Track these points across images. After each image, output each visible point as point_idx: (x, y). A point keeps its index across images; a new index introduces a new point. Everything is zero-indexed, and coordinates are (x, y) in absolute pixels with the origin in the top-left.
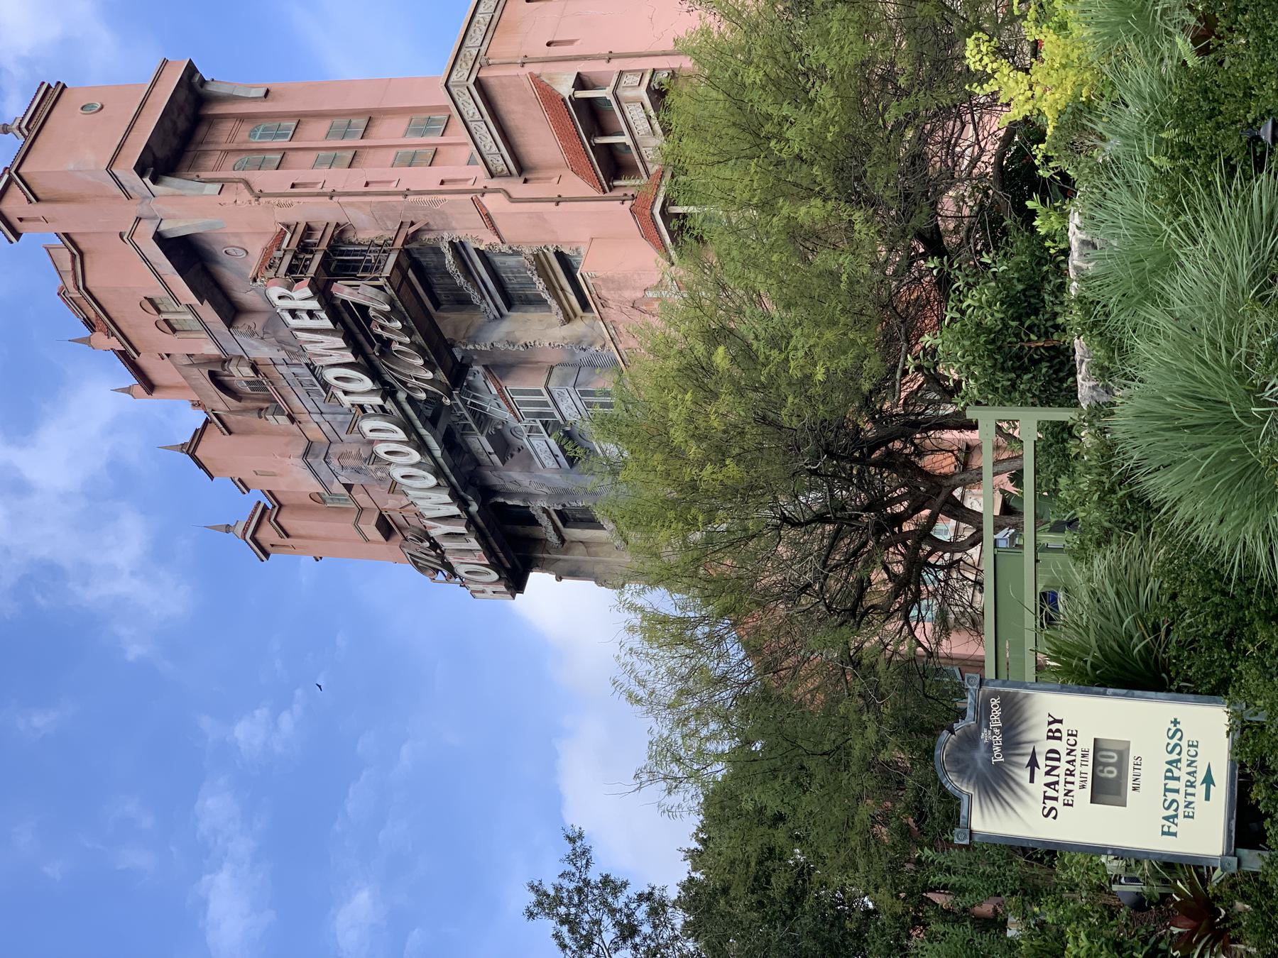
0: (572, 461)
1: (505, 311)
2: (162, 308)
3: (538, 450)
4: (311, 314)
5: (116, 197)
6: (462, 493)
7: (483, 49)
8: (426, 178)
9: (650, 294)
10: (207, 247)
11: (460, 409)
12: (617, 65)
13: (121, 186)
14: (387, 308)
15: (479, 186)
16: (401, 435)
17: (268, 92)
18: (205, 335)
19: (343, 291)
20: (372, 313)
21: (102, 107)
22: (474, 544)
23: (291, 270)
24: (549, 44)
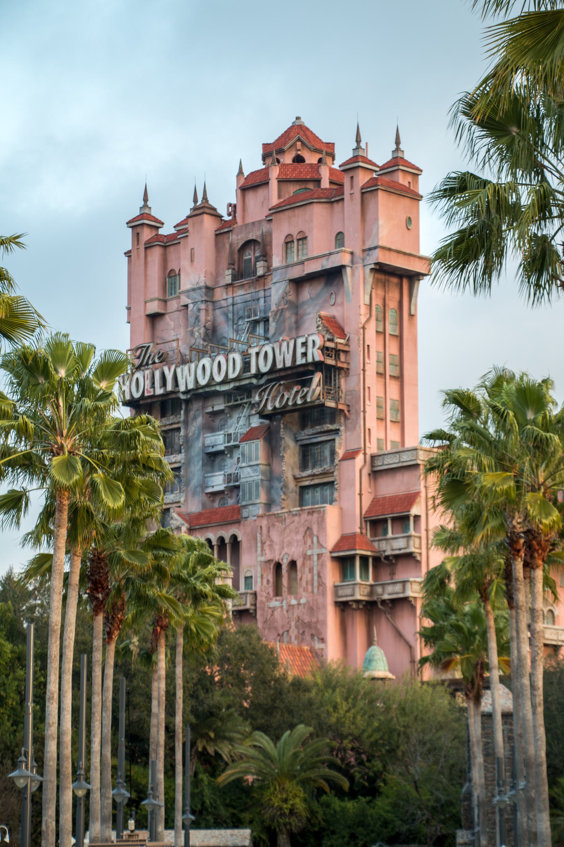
0: (208, 454)
1: (299, 443)
2: (300, 242)
3: (216, 437)
4: (305, 354)
5: (364, 242)
6: (192, 393)
8: (371, 422)
9: (315, 539)
10: (335, 283)
11: (241, 399)
12: (423, 534)
13: (370, 249)
14: (309, 400)
16: (231, 376)
17: (413, 316)
18: (284, 264)
19: (317, 377)
20: (306, 390)
21: (408, 229)
22: (159, 391)
23: (327, 349)
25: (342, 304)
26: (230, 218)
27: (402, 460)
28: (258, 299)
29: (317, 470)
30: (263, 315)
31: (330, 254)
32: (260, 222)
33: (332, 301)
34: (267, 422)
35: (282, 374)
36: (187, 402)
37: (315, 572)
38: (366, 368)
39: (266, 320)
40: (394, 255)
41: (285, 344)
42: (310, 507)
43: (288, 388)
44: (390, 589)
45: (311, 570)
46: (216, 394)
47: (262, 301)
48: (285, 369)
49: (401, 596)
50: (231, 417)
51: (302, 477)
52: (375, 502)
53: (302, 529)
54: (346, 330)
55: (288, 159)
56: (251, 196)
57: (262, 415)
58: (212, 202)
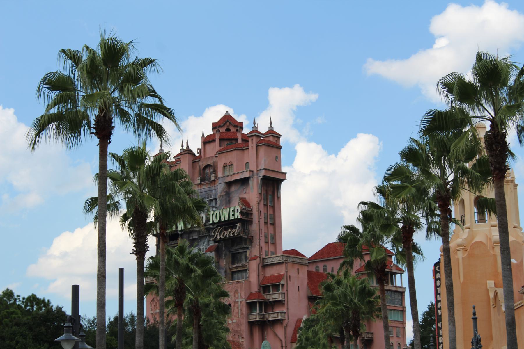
1: (231, 253)
2: (230, 166)
4: (233, 215)
7: (289, 262)
9: (239, 295)
14: (236, 235)
15: (261, 257)
20: (234, 230)
23: (243, 212)
24: (290, 276)
25: (249, 193)
26: (199, 155)
27: (276, 260)
28: (212, 190)
29: (240, 265)
30: (214, 197)
31: (244, 172)
32: (212, 157)
33: (245, 192)
34: (217, 244)
35: (224, 223)
36: (181, 235)
37: (239, 309)
38: (260, 221)
39: (216, 200)
40: (271, 172)
41: (225, 210)
42: (237, 281)
43: (226, 229)
44: (272, 316)
45: (238, 308)
46: (195, 231)
47: (214, 191)
48: (225, 221)
49: (277, 318)
50: (201, 241)
51: (233, 268)
52: (265, 278)
53: (234, 290)
54: (251, 205)
55: (223, 130)
56: (208, 146)
57: (215, 241)
58: (191, 148)
